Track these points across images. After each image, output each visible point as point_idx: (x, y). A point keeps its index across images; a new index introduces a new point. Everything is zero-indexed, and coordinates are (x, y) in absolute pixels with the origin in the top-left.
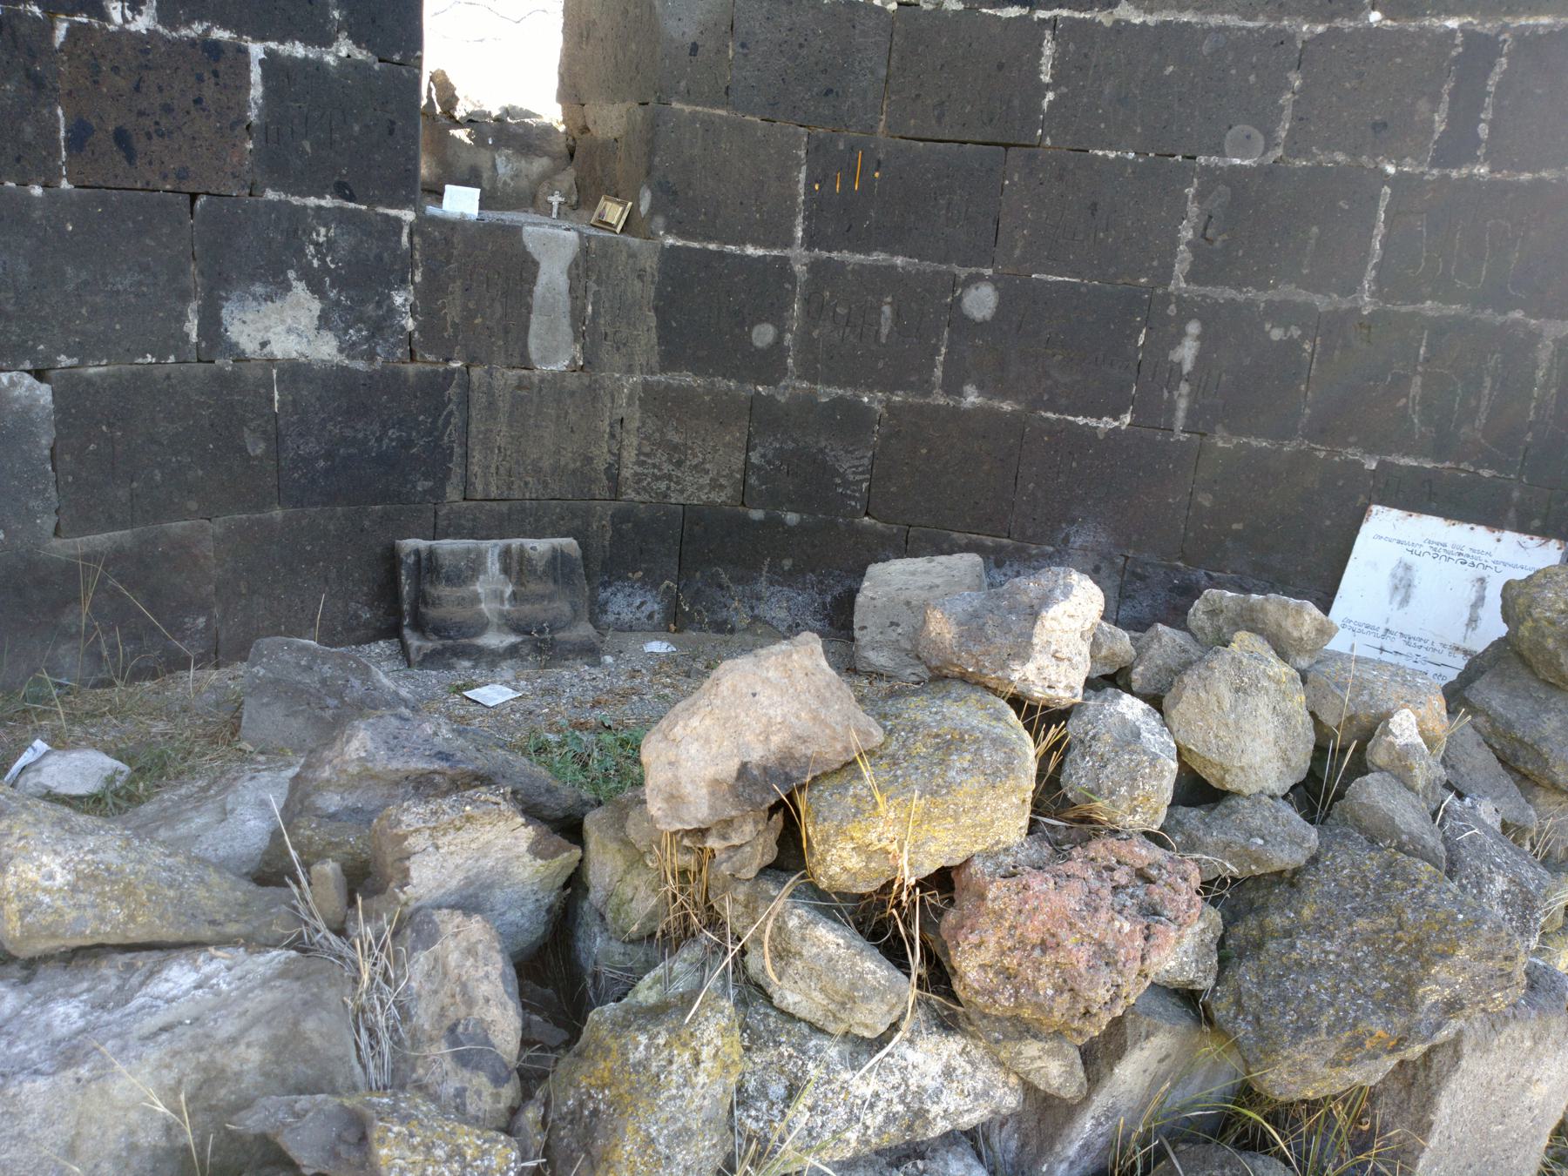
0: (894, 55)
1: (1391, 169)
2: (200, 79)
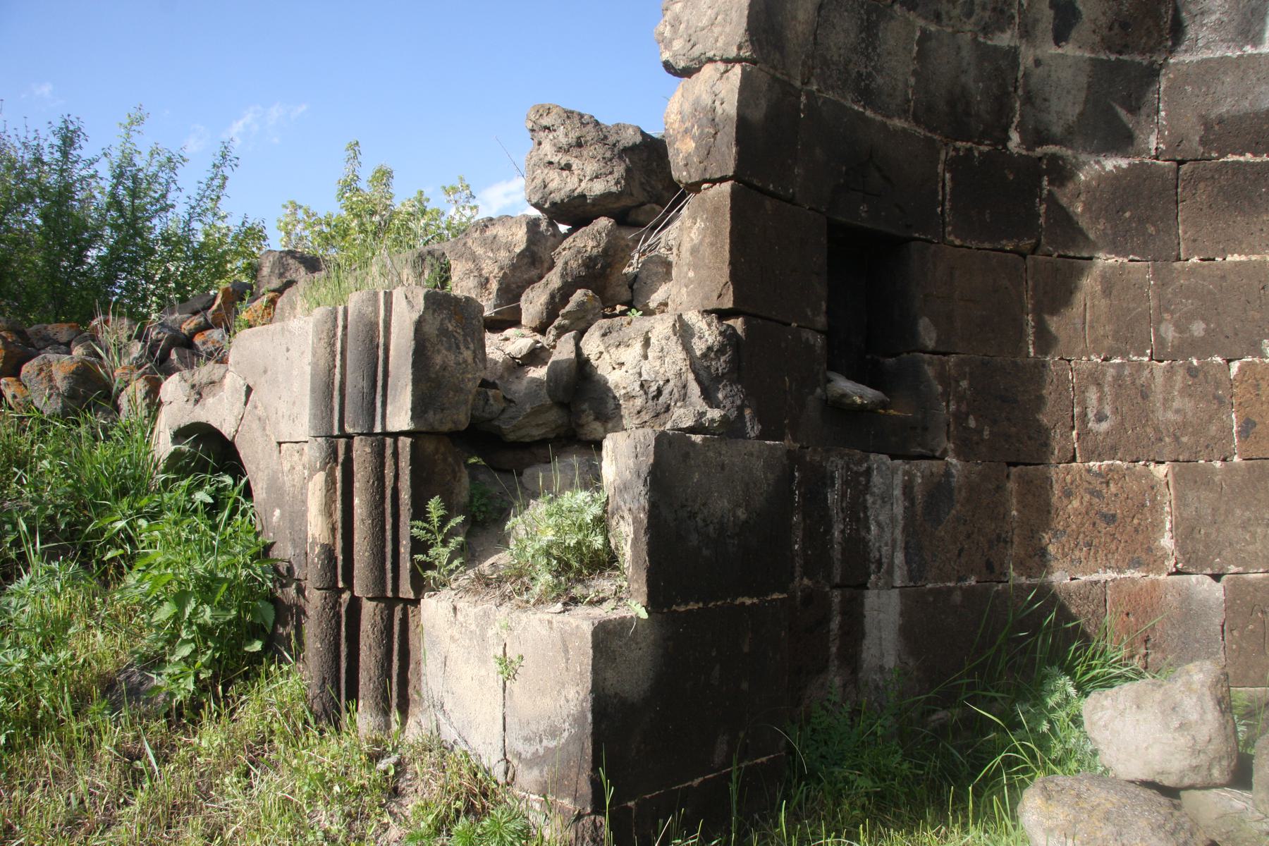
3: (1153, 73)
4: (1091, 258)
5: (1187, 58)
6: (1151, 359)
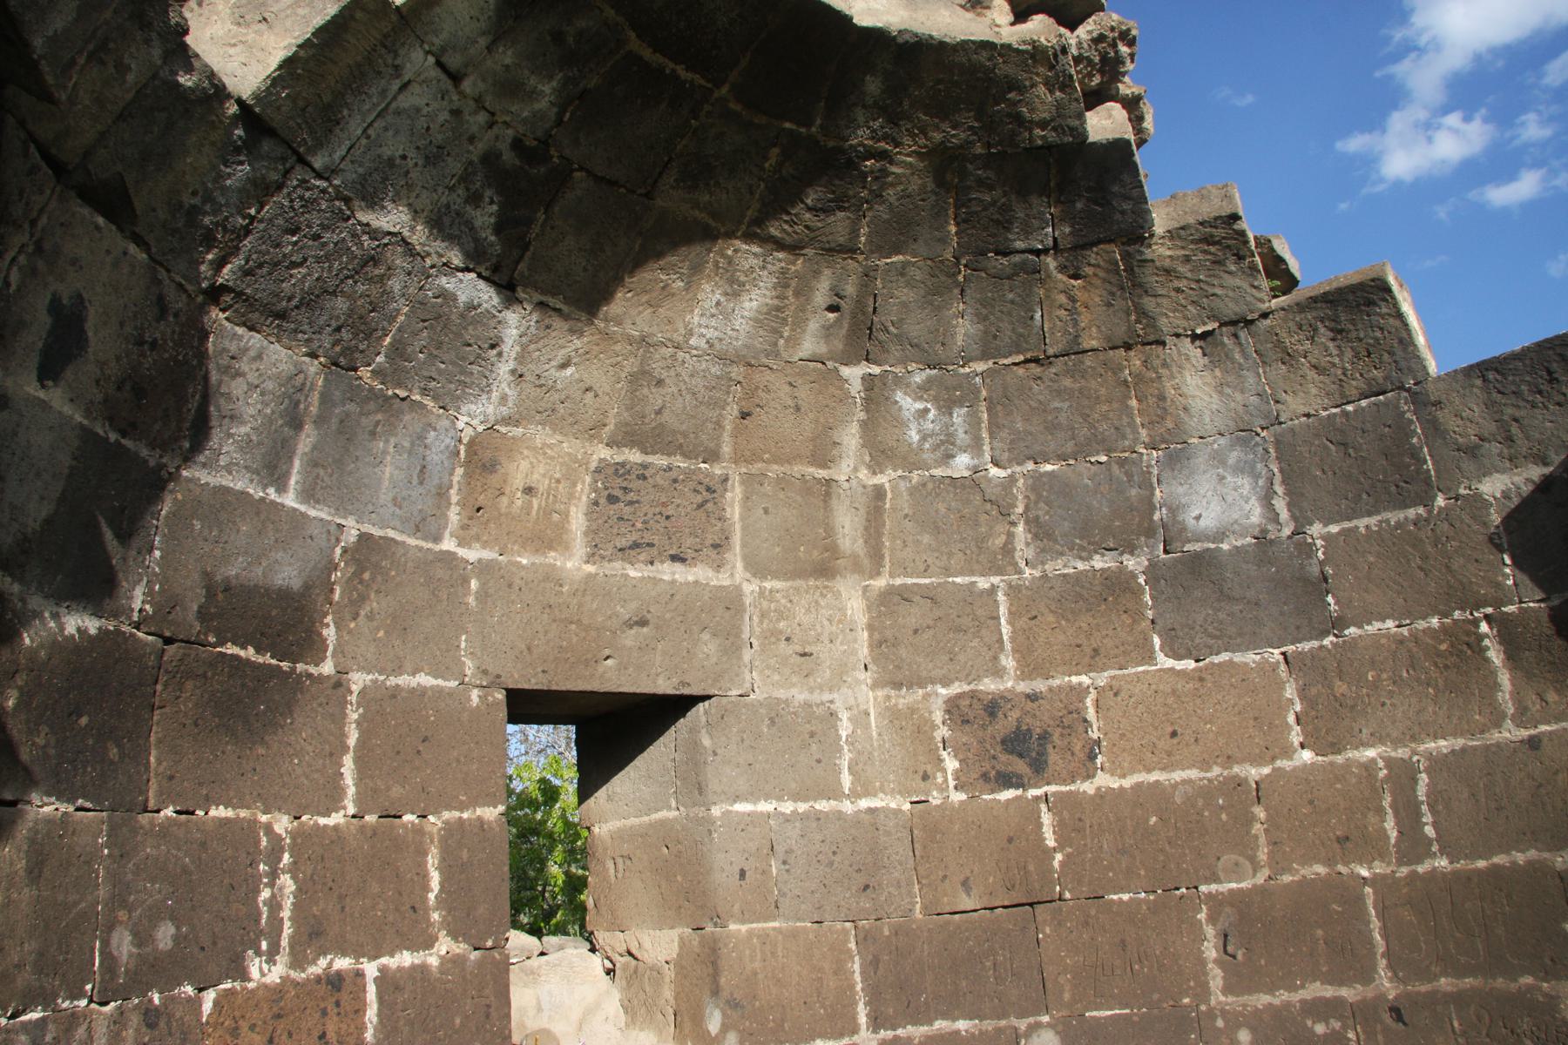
0: (916, 846)
1: (1365, 873)
2: (324, 1013)
3: (156, 483)
4: (14, 804)
5: (204, 477)
6: (91, 1001)
